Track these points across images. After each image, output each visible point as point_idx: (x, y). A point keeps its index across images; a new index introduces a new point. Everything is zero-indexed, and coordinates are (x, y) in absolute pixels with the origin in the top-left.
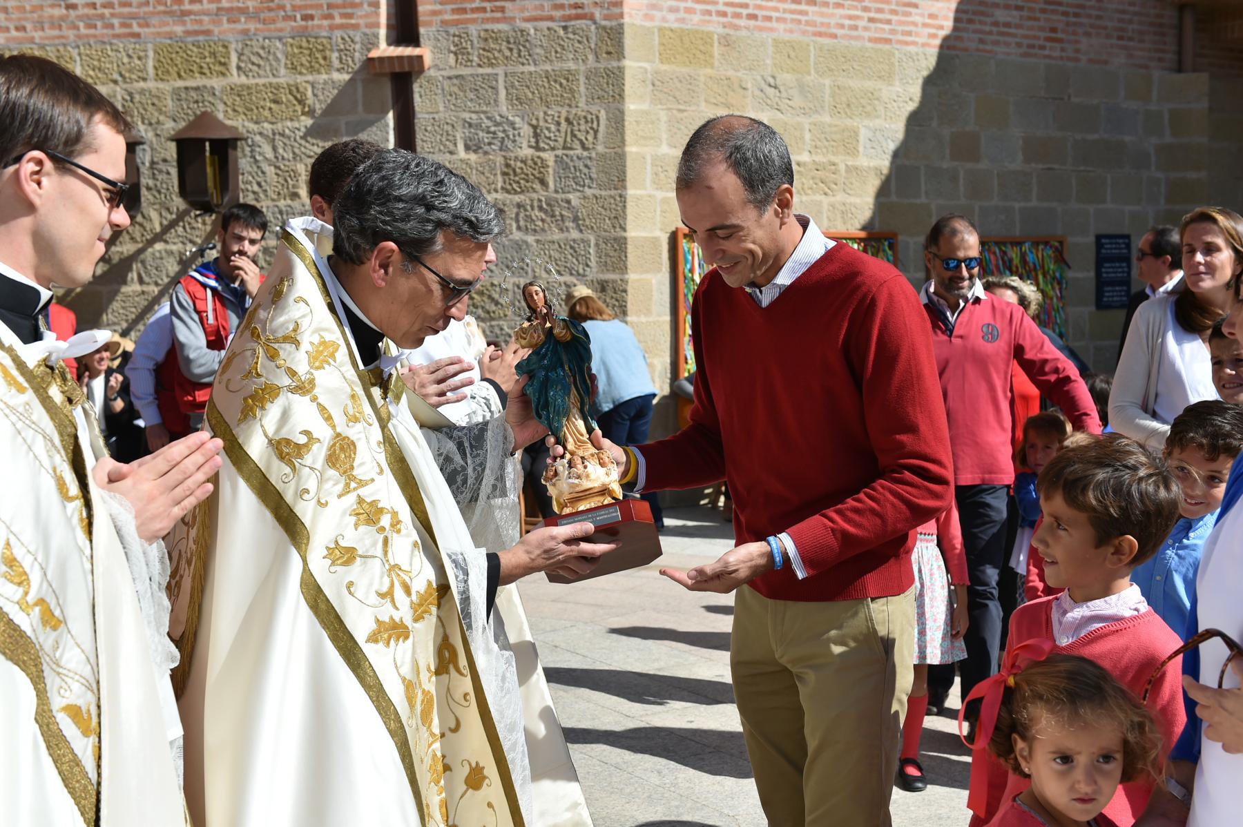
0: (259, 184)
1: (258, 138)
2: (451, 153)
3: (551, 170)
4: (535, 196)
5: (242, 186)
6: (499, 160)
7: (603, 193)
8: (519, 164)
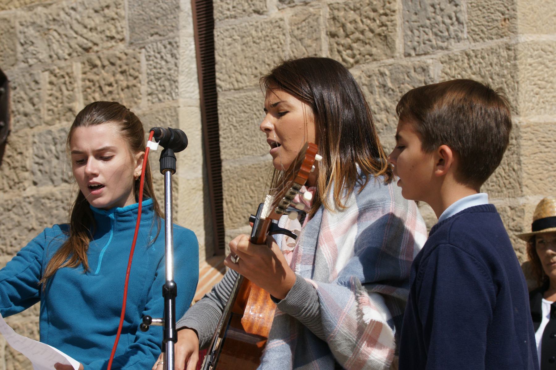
0: (31, 100)
1: (31, 31)
2: (258, 12)
3: (398, 18)
4: (374, 67)
5: (13, 106)
6: (325, 13)
7: (479, 46)
8: (352, 15)
